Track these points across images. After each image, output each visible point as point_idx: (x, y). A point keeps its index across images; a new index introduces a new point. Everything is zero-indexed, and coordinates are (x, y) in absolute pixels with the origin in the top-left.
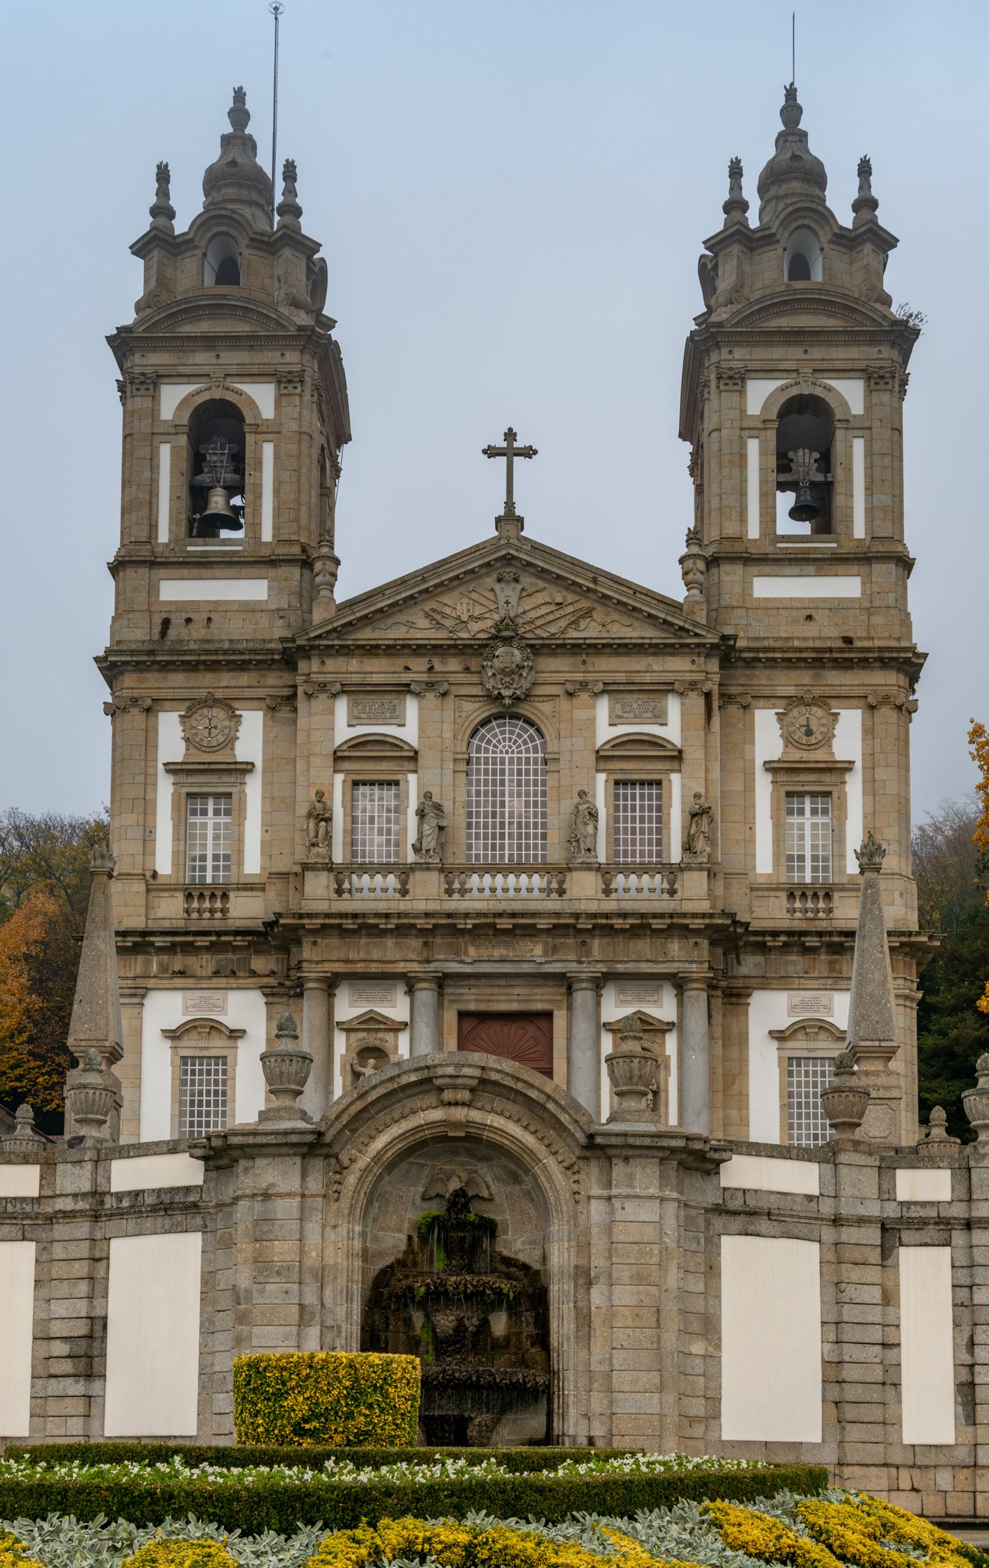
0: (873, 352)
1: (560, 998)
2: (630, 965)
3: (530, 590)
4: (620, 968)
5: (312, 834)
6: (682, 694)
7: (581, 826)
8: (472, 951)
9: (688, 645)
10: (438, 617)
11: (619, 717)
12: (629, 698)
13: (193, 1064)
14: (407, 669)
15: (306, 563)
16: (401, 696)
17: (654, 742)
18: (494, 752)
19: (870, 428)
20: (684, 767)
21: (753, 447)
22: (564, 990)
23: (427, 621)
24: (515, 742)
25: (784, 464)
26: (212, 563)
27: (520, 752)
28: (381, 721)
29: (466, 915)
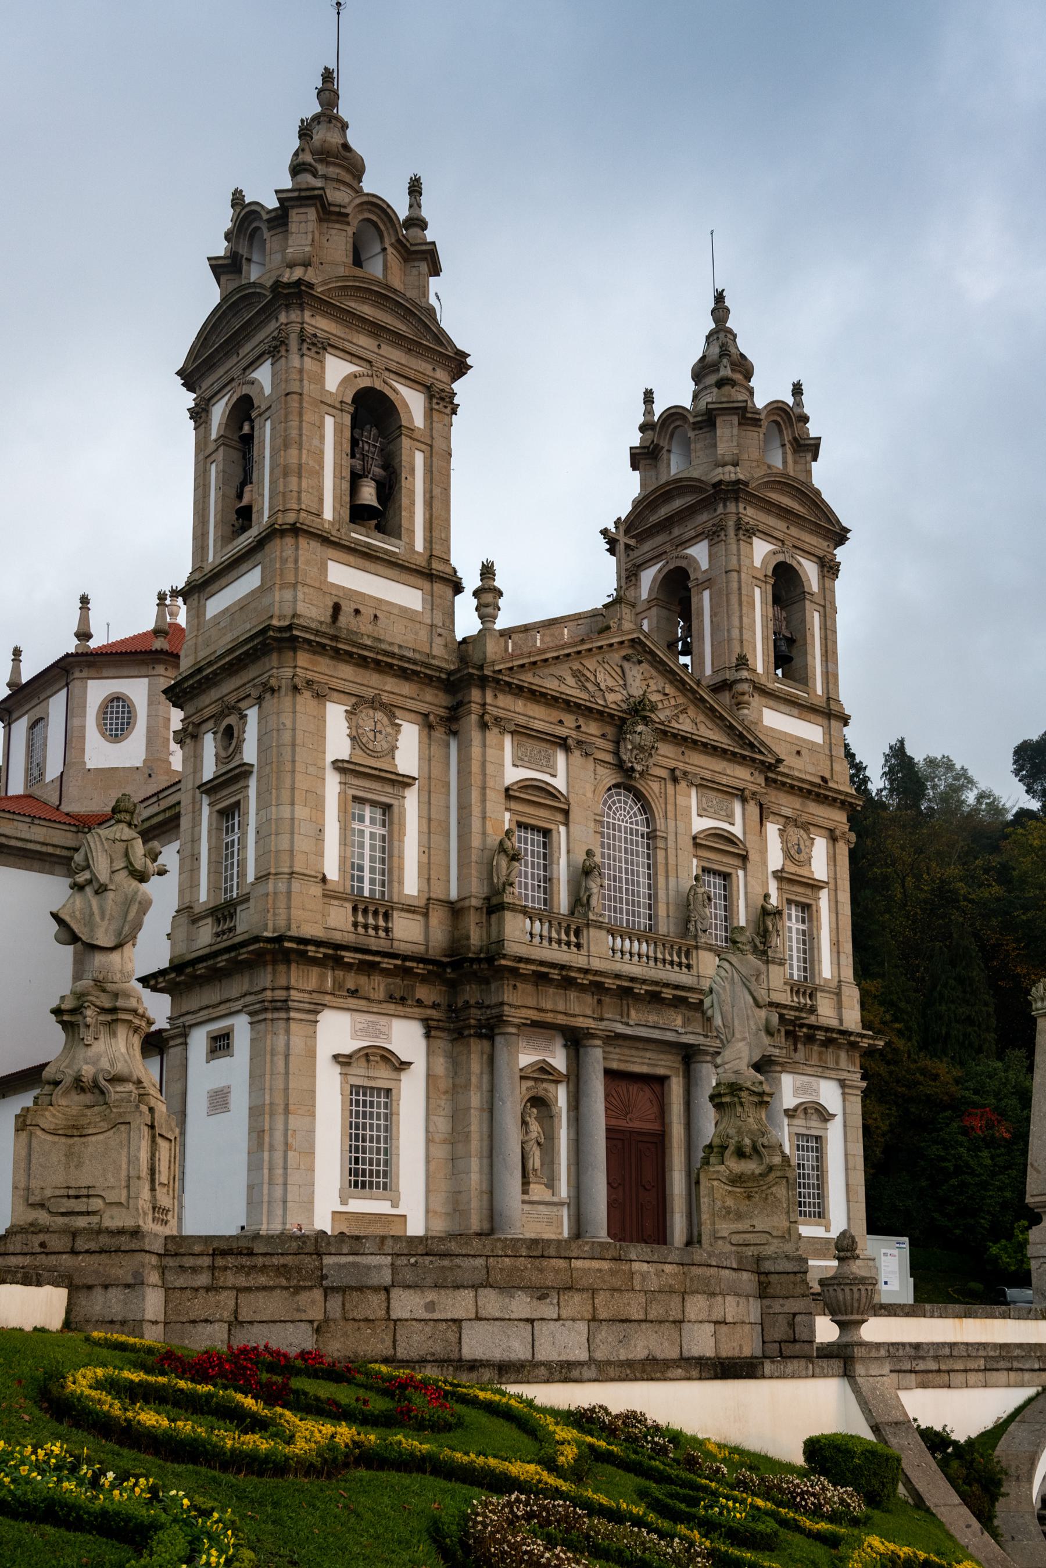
6: (744, 800)
7: (700, 908)
9: (753, 760)
10: (583, 679)
11: (705, 810)
12: (712, 794)
13: (365, 1095)
14: (561, 722)
17: (729, 839)
18: (614, 819)
19: (824, 607)
20: (749, 866)
24: (629, 813)
26: (378, 558)
28: (539, 768)
29: (644, 982)
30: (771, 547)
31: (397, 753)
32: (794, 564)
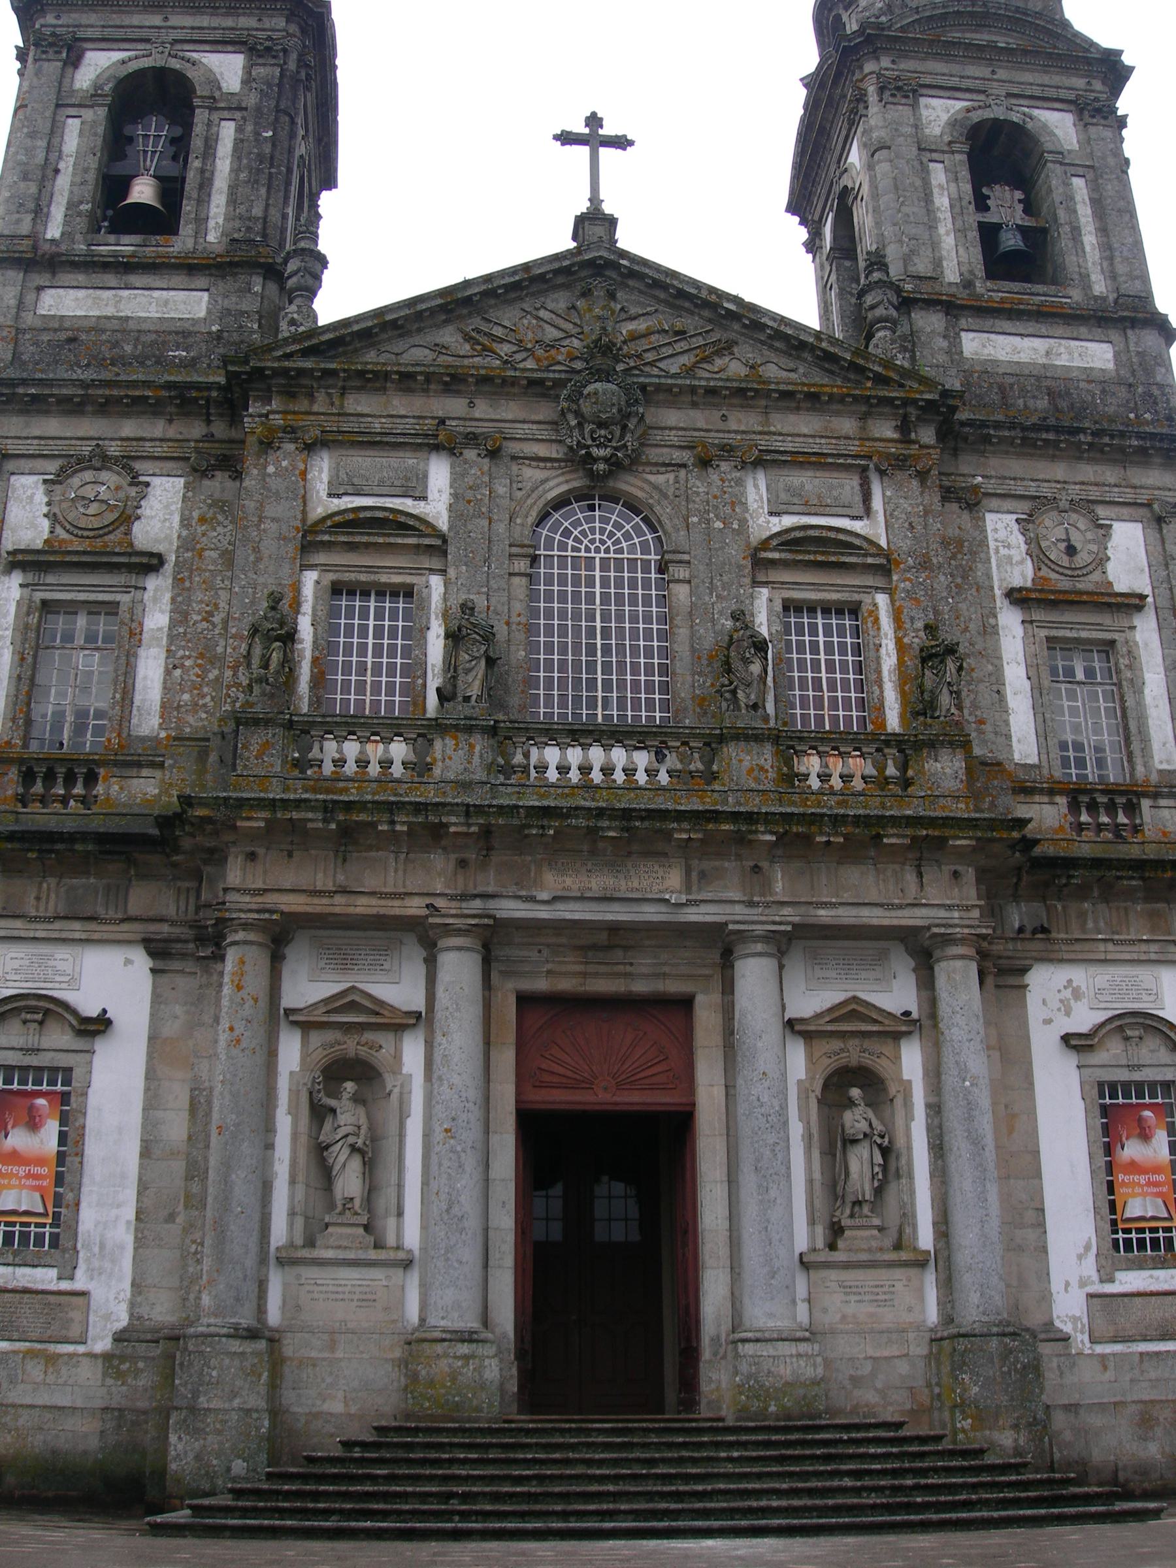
0: (1080, 83)
1: (707, 972)
2: (841, 911)
3: (633, 311)
4: (824, 915)
5: (256, 662)
8: (549, 877)
9: (890, 401)
10: (485, 340)
15: (273, 273)
16: (418, 454)
18: (574, 549)
21: (938, 174)
22: (715, 956)
23: (467, 347)
25: (981, 203)
27: (621, 551)
30: (960, 105)
31: (137, 528)
32: (1015, 118)
